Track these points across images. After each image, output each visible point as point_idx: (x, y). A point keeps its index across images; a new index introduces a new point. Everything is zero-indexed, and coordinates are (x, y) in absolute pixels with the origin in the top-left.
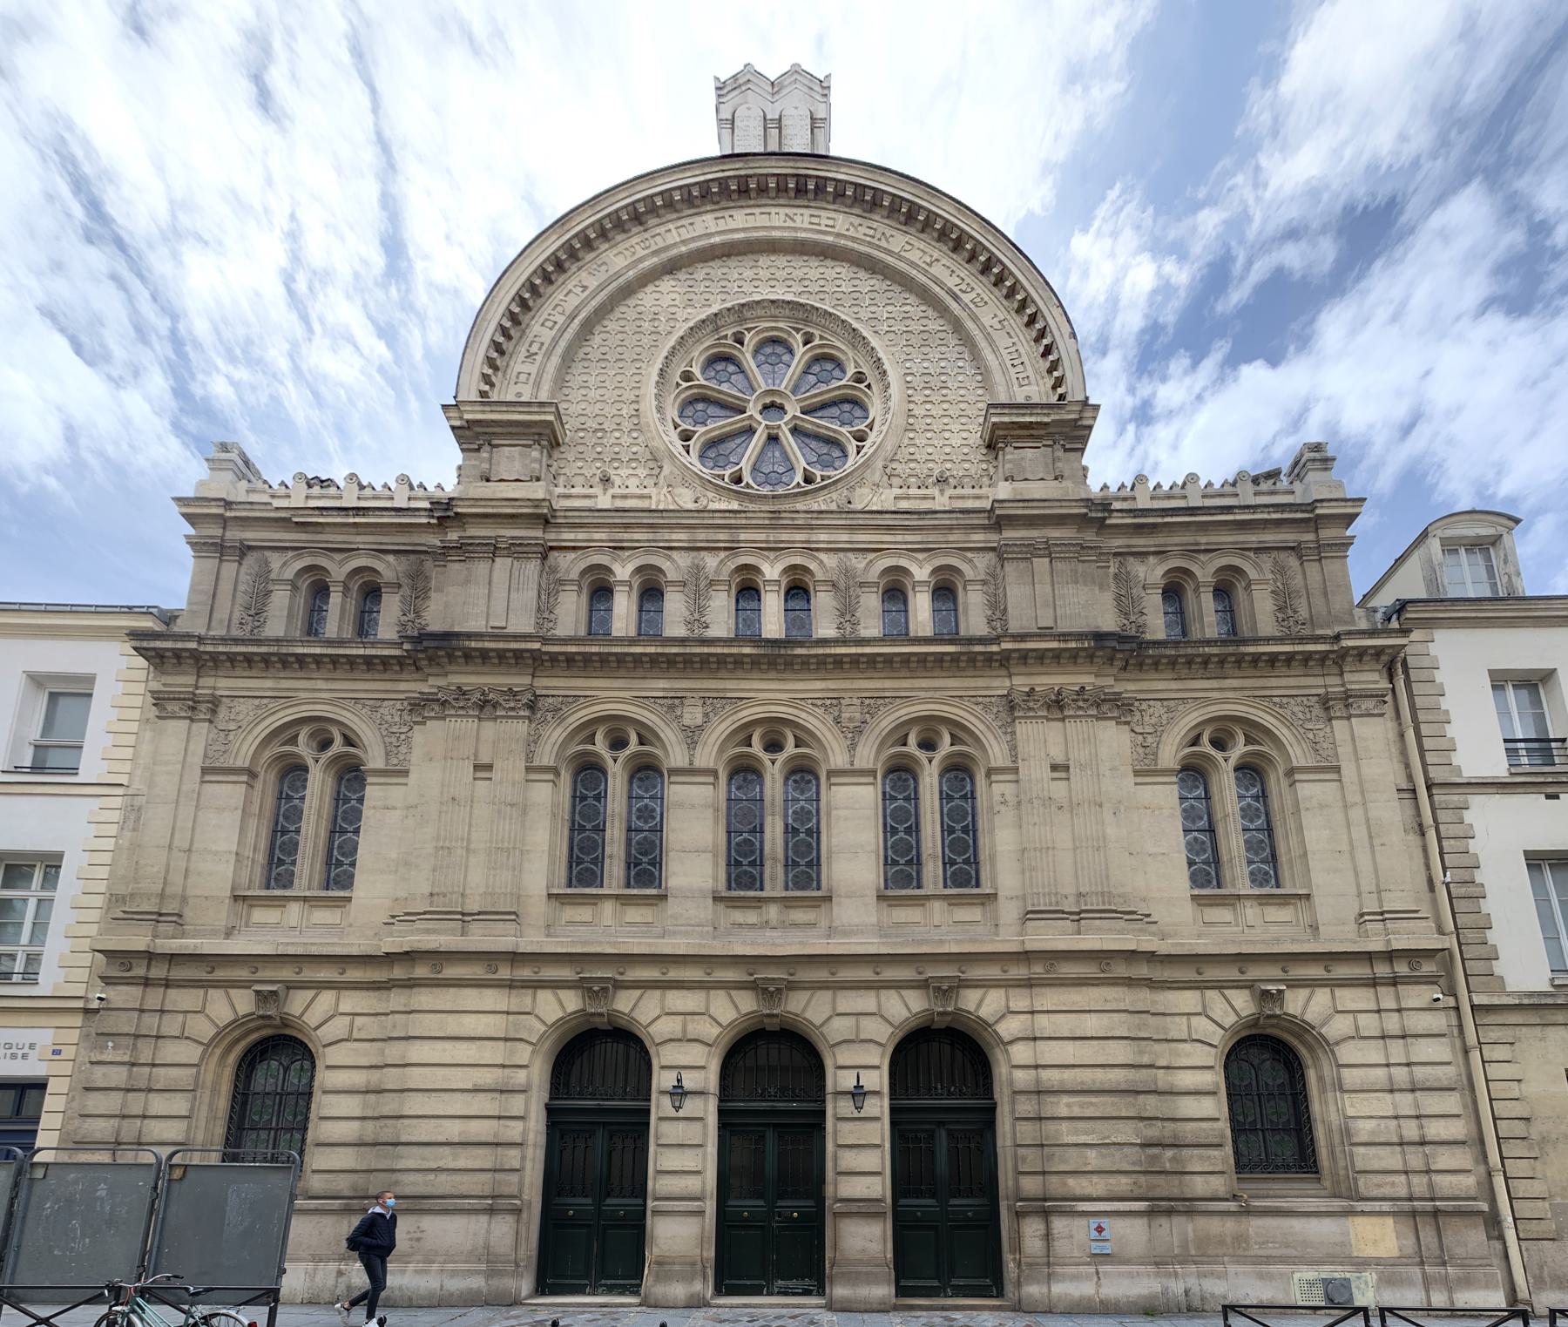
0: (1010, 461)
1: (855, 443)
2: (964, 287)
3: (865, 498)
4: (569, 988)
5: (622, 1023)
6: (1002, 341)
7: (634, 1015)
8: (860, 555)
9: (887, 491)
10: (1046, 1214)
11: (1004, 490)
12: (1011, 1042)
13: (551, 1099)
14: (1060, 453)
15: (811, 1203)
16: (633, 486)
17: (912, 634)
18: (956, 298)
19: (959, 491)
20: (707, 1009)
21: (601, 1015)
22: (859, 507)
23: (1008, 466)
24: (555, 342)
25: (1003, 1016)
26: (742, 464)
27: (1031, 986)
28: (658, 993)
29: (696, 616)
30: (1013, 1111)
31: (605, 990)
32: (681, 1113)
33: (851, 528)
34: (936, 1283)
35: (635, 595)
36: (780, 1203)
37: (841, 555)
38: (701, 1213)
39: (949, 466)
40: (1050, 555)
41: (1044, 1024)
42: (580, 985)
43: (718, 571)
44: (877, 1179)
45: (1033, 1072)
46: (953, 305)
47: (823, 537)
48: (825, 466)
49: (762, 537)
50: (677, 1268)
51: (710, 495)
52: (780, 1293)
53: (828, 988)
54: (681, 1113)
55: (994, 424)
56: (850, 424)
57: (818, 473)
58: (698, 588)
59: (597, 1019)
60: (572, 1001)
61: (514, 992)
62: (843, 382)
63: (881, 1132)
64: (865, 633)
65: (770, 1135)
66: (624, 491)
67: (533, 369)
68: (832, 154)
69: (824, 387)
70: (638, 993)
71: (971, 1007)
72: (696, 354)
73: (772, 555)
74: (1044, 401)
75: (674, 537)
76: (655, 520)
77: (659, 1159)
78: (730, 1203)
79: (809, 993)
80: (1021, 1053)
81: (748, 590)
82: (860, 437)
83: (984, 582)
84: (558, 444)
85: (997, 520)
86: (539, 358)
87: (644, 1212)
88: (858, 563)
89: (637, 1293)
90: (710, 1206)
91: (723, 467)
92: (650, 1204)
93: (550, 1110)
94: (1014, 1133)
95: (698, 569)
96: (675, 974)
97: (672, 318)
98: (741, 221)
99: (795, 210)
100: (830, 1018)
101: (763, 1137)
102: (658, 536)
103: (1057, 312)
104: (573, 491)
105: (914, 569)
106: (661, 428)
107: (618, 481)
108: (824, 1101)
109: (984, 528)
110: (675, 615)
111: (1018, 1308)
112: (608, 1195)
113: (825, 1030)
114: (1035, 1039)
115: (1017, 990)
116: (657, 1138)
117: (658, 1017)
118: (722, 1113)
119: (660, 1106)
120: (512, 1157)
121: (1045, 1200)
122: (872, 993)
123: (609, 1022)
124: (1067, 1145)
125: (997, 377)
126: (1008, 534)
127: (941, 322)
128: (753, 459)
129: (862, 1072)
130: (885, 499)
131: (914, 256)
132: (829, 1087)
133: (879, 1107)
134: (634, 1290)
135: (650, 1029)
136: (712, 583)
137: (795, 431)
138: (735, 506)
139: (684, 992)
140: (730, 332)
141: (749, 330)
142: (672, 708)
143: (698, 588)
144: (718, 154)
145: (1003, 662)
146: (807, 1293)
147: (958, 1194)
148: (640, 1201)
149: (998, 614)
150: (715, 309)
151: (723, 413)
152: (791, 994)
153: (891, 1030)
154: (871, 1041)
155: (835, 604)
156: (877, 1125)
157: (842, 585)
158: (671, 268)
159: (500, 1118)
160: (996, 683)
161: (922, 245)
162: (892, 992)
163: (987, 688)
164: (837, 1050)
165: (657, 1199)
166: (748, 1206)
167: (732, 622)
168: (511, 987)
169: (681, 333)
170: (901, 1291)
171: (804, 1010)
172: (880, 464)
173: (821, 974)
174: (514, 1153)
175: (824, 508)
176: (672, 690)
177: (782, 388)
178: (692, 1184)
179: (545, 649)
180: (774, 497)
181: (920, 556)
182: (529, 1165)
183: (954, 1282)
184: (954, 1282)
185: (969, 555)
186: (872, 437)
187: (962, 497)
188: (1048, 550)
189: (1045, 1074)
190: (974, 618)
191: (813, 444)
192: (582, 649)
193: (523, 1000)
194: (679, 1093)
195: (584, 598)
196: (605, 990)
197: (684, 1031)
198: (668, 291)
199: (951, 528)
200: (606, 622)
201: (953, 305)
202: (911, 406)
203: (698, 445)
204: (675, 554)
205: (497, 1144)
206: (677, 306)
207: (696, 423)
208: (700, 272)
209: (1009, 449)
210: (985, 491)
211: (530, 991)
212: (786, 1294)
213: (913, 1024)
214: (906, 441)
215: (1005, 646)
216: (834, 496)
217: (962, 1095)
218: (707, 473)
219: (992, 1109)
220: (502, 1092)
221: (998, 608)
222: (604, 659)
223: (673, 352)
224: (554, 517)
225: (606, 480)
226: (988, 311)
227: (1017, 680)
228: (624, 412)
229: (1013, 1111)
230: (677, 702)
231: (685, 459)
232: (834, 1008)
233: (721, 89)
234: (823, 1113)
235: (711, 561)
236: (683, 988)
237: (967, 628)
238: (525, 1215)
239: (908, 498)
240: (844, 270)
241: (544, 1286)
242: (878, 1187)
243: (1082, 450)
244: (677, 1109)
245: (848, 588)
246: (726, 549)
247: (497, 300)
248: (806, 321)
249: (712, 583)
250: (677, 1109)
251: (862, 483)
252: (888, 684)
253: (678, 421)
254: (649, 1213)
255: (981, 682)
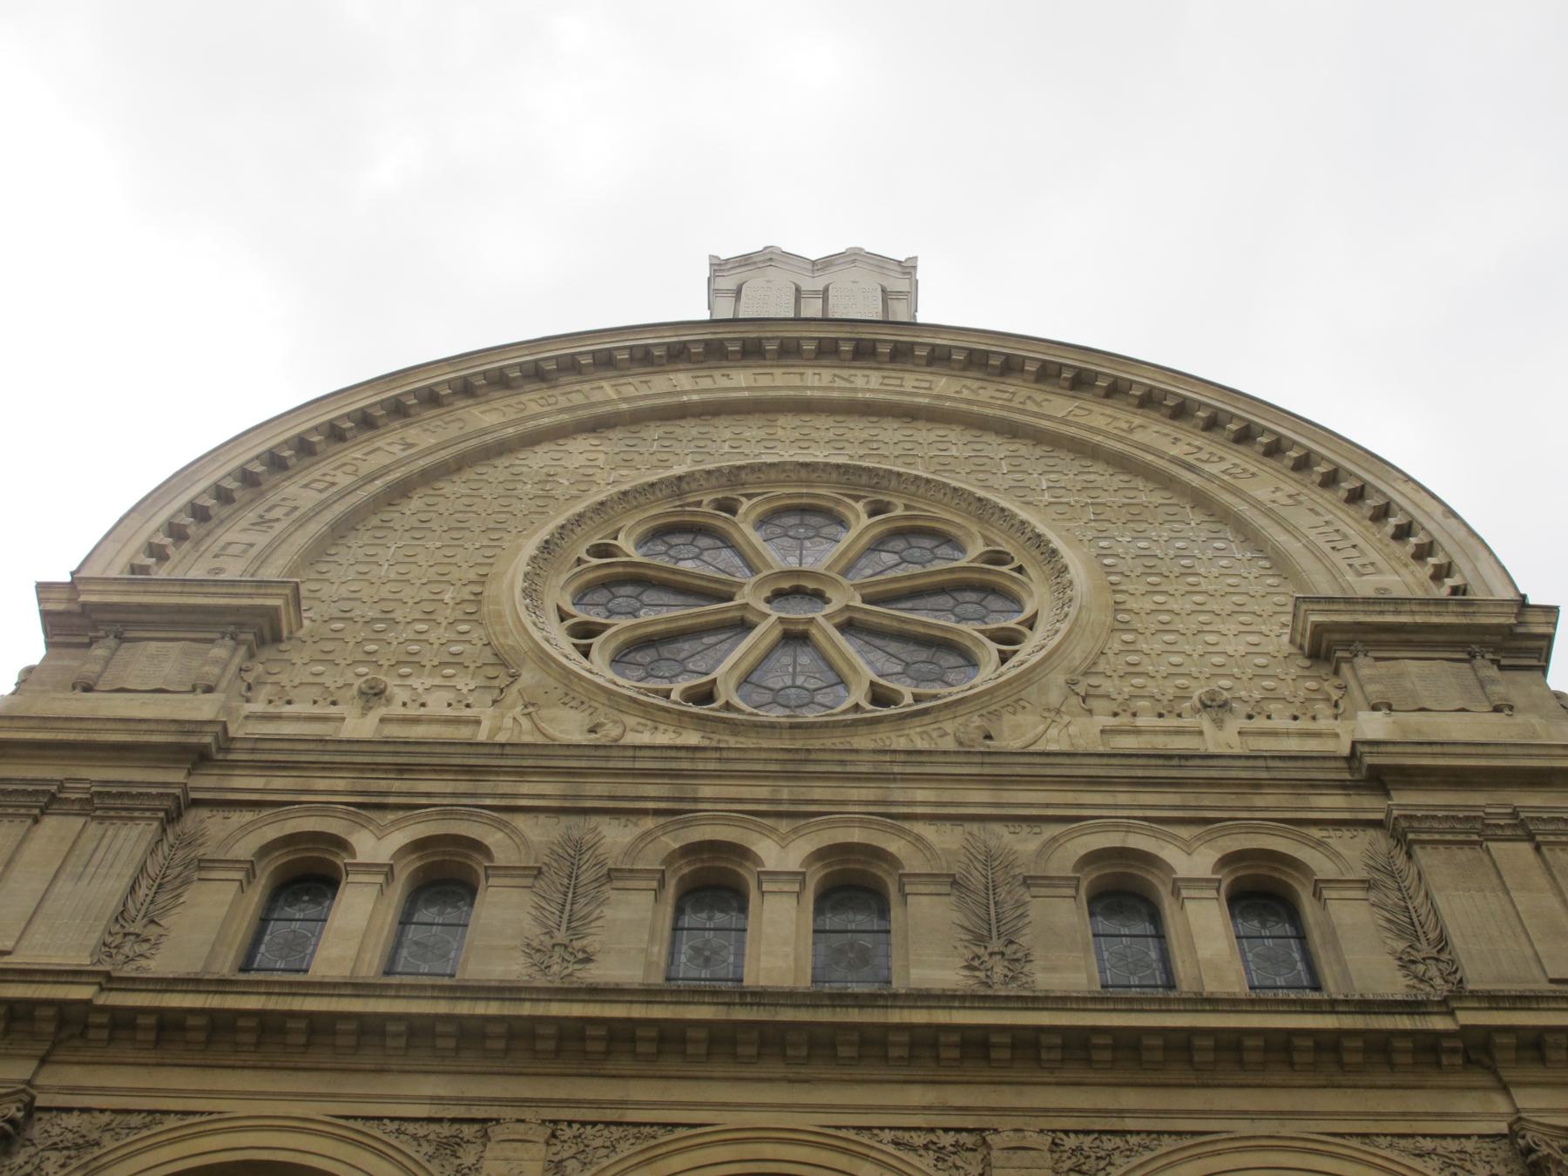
0: (1372, 680)
1: (993, 647)
2: (1205, 457)
3: (1019, 731)
6: (1303, 520)
8: (1025, 829)
9: (1084, 720)
11: (1373, 726)
14: (1493, 672)
16: (431, 703)
17: (1186, 986)
18: (1190, 468)
19: (1260, 723)
22: (1015, 745)
23: (1370, 688)
24: (324, 506)
26: (718, 673)
29: (561, 936)
33: (997, 781)
35: (397, 892)
37: (974, 827)
39: (1225, 683)
40: (1530, 837)
43: (632, 850)
46: (1187, 476)
47: (920, 795)
48: (919, 679)
49: (762, 792)
51: (631, 721)
55: (1316, 625)
56: (982, 619)
57: (906, 690)
58: (573, 883)
62: (962, 563)
64: (1044, 980)
66: (413, 711)
67: (262, 540)
68: (921, 319)
69: (918, 569)
72: (629, 523)
73: (784, 826)
74: (1420, 594)
75: (525, 788)
76: (480, 762)
81: (713, 886)
82: (1008, 639)
83: (1368, 885)
84: (277, 638)
85: (1372, 773)
86: (278, 527)
88: (1024, 844)
91: (671, 679)
95: (577, 850)
97: (588, 479)
98: (740, 381)
99: (853, 372)
102: (485, 787)
103: (1408, 489)
104: (287, 709)
105: (1169, 853)
106: (527, 619)
107: (401, 695)
109: (1343, 786)
110: (499, 939)
125: (1305, 561)
126: (1406, 799)
127: (1167, 494)
128: (744, 667)
130: (1081, 732)
131: (1099, 421)
136: (611, 875)
137: (849, 626)
138: (692, 738)
140: (707, 499)
141: (749, 496)
142: (450, 1146)
143: (573, 883)
144: (706, 316)
145: (1478, 1055)
149: (1426, 949)
150: (678, 470)
151: (680, 599)
155: (956, 916)
157: (977, 880)
158: (597, 425)
160: (1467, 1103)
161: (1109, 411)
163: (1441, 1116)
167: (659, 951)
169: (601, 497)
172: (1059, 678)
175: (921, 744)
176: (458, 1101)
177: (820, 568)
179: (103, 999)
180: (793, 726)
181: (1185, 832)
185: (1316, 833)
186: (1033, 640)
187: (1274, 734)
188: (1523, 829)
190: (1361, 955)
191: (893, 647)
192: (214, 1002)
195: (256, 896)
198: (579, 451)
199: (1256, 785)
200: (301, 948)
201: (1187, 476)
202: (1120, 598)
203: (613, 645)
204: (520, 821)
206: (596, 469)
207: (611, 613)
208: (654, 432)
209: (1360, 660)
210: (1324, 724)
214: (1117, 646)
215: (1466, 1018)
216: (949, 726)
218: (627, 685)
221: (1421, 938)
222: (270, 1027)
223: (579, 519)
224: (228, 750)
225: (374, 694)
226: (1264, 487)
227: (1529, 1100)
228: (447, 597)
230: (468, 1131)
231: (576, 663)
233: (719, 267)
235: (615, 836)
237: (1345, 972)
239: (1137, 732)
240: (954, 434)
243: (1544, 669)
245: (991, 887)
246: (657, 812)
247: (223, 459)
248: (875, 488)
249: (611, 875)
251: (1017, 705)
252: (1130, 1099)
253: (569, 607)
255: (1418, 1101)
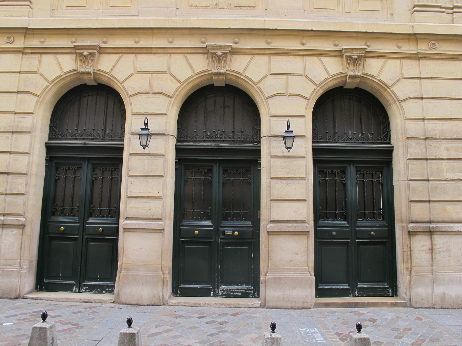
4: (66, 53)
5: (104, 80)
7: (113, 73)
10: (431, 233)
12: (405, 100)
13: (50, 139)
15: (249, 224)
20: (169, 68)
21: (89, 73)
25: (399, 80)
27: (419, 59)
28: (132, 56)
30: (406, 153)
31: (92, 54)
32: (147, 151)
34: (346, 286)
36: (224, 224)
38: (161, 230)
41: (429, 88)
42: (75, 50)
44: (302, 205)
45: (421, 123)
50: (142, 273)
52: (223, 296)
53: (264, 54)
54: (147, 151)
59: (86, 77)
60: (68, 64)
61: (25, 56)
63: (305, 168)
65: (216, 169)
70: (117, 56)
71: (374, 73)
77: (129, 187)
78: (185, 223)
79: (249, 57)
80: (413, 109)
87: (118, 228)
89: (111, 292)
90: (169, 225)
92: (123, 223)
93: (49, 148)
94: (407, 169)
96: (144, 42)
100: (266, 76)
101: (210, 171)
108: (259, 142)
111: (408, 304)
112: (91, 216)
113: (261, 85)
114: (422, 98)
115: (409, 61)
116: (128, 170)
117: (132, 75)
118: (178, 150)
119: (131, 144)
120: (19, 184)
121: (430, 222)
122: (299, 59)
123: (95, 79)
124: (446, 180)
129: (290, 119)
132: (264, 131)
133: (304, 148)
134: (110, 290)
135: (124, 84)
139: (151, 56)
146: (245, 295)
147: (364, 217)
148: (114, 220)
152: (234, 57)
153: (315, 87)
154: (298, 95)
156: (302, 162)
159: (11, 153)
162: (315, 59)
164: (270, 101)
165: (127, 219)
166: (198, 225)
168: (23, 53)
170: (320, 293)
171: (245, 70)
173: (259, 44)
174: (20, 180)
178: (154, 208)
182: (32, 190)
183: (360, 285)
184: (360, 285)
189: (430, 125)
193: (30, 62)
194: (146, 134)
196: (92, 54)
197: (151, 85)
205: (8, 174)
211: (37, 56)
212: (228, 296)
213: (330, 84)
217: (367, 140)
219: (390, 152)
220: (13, 133)
229: (406, 153)
232: (269, 69)
234: (258, 152)
236: (151, 53)
238: (28, 229)
241: (42, 284)
242: (304, 212)
244: (144, 146)
250: (144, 146)
254: (121, 230)
